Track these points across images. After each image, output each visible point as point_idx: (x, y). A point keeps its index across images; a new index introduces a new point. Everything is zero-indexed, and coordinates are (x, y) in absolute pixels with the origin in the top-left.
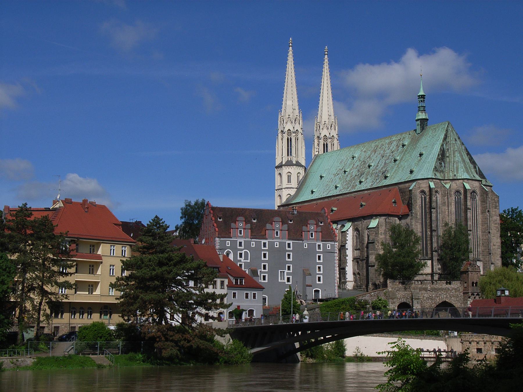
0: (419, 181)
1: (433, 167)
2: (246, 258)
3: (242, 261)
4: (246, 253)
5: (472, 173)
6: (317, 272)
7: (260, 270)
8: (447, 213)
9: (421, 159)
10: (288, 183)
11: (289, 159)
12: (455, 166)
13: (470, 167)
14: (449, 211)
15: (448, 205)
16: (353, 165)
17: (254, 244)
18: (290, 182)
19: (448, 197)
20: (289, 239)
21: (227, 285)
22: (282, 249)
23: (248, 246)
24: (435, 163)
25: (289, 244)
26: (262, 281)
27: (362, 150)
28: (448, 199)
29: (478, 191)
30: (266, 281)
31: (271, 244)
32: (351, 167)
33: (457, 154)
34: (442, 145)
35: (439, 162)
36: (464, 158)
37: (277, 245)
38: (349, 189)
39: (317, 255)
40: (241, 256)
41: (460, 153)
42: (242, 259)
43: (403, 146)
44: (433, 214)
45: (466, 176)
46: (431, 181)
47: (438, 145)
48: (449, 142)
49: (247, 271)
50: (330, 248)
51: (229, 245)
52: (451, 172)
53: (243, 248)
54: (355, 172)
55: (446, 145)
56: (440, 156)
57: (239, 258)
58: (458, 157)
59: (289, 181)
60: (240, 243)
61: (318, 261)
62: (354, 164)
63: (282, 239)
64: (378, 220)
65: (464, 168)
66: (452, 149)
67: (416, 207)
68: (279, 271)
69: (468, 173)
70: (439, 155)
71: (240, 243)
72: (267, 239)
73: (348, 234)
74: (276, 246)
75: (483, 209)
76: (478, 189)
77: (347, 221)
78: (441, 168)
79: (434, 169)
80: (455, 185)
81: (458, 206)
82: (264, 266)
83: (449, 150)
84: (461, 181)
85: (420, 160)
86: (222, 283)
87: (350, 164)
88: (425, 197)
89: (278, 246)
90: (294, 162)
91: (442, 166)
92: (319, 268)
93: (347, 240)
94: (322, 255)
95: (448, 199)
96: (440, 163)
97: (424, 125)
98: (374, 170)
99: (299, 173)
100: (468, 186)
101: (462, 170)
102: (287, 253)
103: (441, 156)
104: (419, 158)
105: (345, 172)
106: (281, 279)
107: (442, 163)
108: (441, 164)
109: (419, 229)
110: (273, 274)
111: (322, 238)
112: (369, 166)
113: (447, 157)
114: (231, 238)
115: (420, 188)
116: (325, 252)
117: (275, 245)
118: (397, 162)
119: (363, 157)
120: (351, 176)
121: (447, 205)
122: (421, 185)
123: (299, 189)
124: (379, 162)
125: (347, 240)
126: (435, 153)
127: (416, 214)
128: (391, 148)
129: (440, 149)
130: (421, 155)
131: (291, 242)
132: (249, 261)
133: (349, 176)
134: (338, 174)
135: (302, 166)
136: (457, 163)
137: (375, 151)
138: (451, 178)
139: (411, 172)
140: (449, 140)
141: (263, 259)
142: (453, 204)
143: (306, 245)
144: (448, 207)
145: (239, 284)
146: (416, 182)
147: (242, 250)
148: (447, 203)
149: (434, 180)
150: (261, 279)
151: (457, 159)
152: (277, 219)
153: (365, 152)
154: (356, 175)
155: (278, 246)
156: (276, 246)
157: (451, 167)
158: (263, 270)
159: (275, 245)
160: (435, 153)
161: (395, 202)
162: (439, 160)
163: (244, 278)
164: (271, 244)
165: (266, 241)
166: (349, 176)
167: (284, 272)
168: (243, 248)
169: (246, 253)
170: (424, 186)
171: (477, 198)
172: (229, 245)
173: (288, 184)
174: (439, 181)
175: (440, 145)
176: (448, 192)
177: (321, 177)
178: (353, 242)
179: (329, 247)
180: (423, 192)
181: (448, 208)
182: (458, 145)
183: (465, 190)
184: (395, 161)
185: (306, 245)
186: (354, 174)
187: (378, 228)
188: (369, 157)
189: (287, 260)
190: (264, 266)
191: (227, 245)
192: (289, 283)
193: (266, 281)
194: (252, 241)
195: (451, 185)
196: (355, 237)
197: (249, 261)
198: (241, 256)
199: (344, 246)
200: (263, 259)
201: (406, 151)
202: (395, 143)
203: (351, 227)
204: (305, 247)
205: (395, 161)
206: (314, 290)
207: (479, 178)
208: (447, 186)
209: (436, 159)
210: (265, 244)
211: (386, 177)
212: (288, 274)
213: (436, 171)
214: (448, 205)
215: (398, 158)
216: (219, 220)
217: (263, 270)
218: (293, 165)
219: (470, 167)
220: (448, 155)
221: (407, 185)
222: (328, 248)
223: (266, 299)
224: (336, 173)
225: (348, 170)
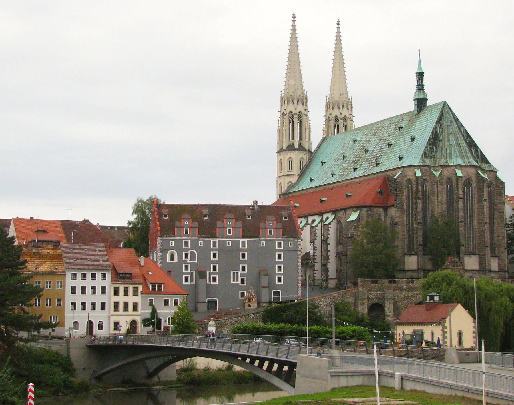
0: (406, 169)
1: (422, 153)
2: (193, 259)
4: (193, 254)
5: (468, 158)
8: (436, 203)
9: (412, 143)
10: (290, 169)
11: (291, 144)
12: (448, 151)
13: (466, 152)
14: (439, 201)
15: (438, 194)
16: (352, 150)
18: (292, 169)
19: (437, 186)
20: (244, 237)
21: (141, 292)
22: (235, 249)
23: (194, 245)
24: (424, 148)
25: (244, 243)
26: (212, 283)
27: (364, 133)
28: (437, 188)
29: (474, 178)
30: (217, 283)
31: (222, 244)
32: (350, 152)
33: (452, 138)
34: (435, 128)
35: (430, 146)
36: (460, 141)
37: (229, 243)
38: (343, 177)
39: (277, 254)
40: (187, 256)
41: (455, 136)
42: (188, 260)
43: (400, 128)
44: (418, 205)
45: (460, 162)
46: (418, 169)
47: (431, 127)
48: (444, 124)
49: (194, 273)
50: (292, 246)
52: (443, 157)
53: (189, 248)
54: (352, 158)
55: (440, 128)
56: (432, 140)
57: (184, 259)
58: (452, 141)
59: (291, 167)
60: (186, 243)
61: (277, 260)
62: (354, 149)
63: (235, 237)
64: (358, 213)
65: (458, 154)
66: (446, 132)
67: (402, 197)
69: (462, 157)
70: (430, 139)
71: (186, 243)
72: (215, 237)
73: (330, 228)
74: (227, 245)
75: (479, 198)
76: (474, 176)
77: (331, 213)
78: (432, 154)
79: (423, 155)
80: (447, 173)
81: (450, 196)
83: (443, 133)
84: (453, 168)
85: (411, 145)
86: (136, 290)
87: (351, 149)
88: (411, 186)
89: (230, 245)
90: (296, 146)
91: (434, 152)
92: (280, 268)
93: (329, 234)
94: (282, 254)
95: (437, 188)
96: (430, 148)
97: (422, 105)
98: (369, 156)
99: (302, 158)
100: (459, 173)
101: (455, 155)
102: (241, 253)
103: (433, 140)
104: (411, 142)
105: (344, 157)
106: (234, 281)
107: (433, 148)
108: (432, 149)
109: (405, 222)
110: (225, 275)
111: (283, 235)
112: (366, 151)
113: (440, 141)
115: (406, 176)
116: (287, 250)
118: (392, 146)
119: (363, 140)
120: (349, 162)
121: (436, 194)
122: (408, 173)
123: (301, 176)
124: (376, 146)
125: (329, 234)
126: (426, 137)
127: (402, 205)
128: (390, 130)
129: (432, 132)
130: (413, 139)
131: (246, 240)
133: (347, 162)
134: (338, 160)
135: (305, 150)
136: (451, 147)
137: (375, 134)
138: (442, 164)
139: (401, 158)
140: (444, 122)
141: (212, 259)
142: (444, 193)
143: (263, 244)
144: (438, 196)
145: (157, 290)
146: (402, 169)
147: (188, 250)
148: (436, 192)
149: (422, 167)
150: (210, 281)
151: (451, 143)
152: (229, 216)
153: (366, 135)
154: (353, 161)
155: (230, 245)
156: (227, 245)
157: (443, 152)
158: (212, 271)
160: (426, 137)
161: (380, 192)
162: (430, 144)
163: (163, 283)
164: (222, 244)
165: (217, 240)
166: (347, 162)
167: (237, 273)
168: (189, 248)
169: (193, 254)
170: (411, 174)
171: (473, 186)
173: (290, 170)
174: (428, 168)
175: (432, 129)
176: (437, 180)
177: (323, 163)
178: (337, 236)
179: (291, 245)
180: (409, 180)
181: (438, 198)
182: (454, 127)
183: (458, 178)
184: (390, 145)
185: (263, 244)
186: (352, 160)
187: (359, 221)
188: (369, 140)
189: (241, 259)
192: (243, 285)
193: (217, 283)
195: (441, 172)
196: (338, 231)
197: (196, 262)
198: (187, 256)
199: (326, 240)
200: (212, 259)
201: (401, 134)
202: (394, 126)
203: (334, 219)
205: (390, 145)
206: (279, 292)
207: (474, 163)
208: (437, 174)
209: (426, 143)
210: (215, 243)
211: (378, 164)
212: (242, 275)
213: (425, 157)
214: (438, 194)
215: (393, 142)
217: (212, 271)
218: (295, 150)
219: (466, 152)
220: (441, 138)
221: (395, 172)
222: (289, 246)
223: (216, 302)
224: (337, 159)
225: (347, 155)
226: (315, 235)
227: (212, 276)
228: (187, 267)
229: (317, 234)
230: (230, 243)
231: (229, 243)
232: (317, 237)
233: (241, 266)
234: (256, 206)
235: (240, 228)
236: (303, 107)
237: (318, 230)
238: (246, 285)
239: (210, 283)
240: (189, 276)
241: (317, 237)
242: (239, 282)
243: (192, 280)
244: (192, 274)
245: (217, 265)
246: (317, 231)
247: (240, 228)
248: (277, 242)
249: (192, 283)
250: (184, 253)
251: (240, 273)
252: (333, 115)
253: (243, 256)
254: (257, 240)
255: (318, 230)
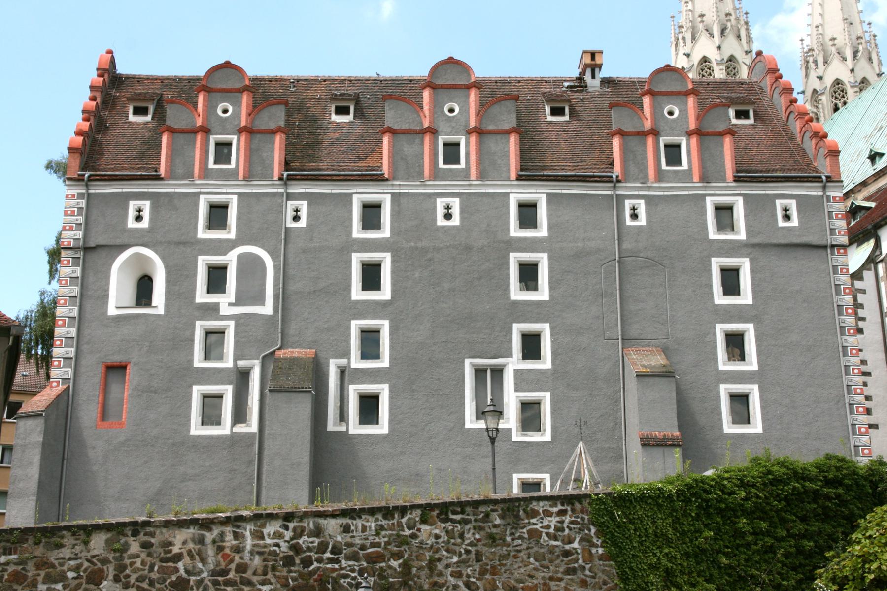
3: (225, 310)
6: (722, 367)
7: (343, 362)
17: (303, 214)
26: (355, 427)
30: (383, 427)
39: (716, 264)
51: (145, 224)
57: (202, 296)
61: (720, 299)
68: (468, 362)
74: (441, 222)
82: (370, 339)
92: (735, 342)
114: (158, 178)
117: (440, 211)
131: (538, 194)
132: (267, 309)
141: (357, 293)
150: (343, 417)
155: (456, 221)
156: (441, 222)
158: (356, 362)
159: (440, 211)
165: (382, 196)
167: (498, 372)
172: (145, 224)
189: (517, 293)
190: (370, 339)
191: (131, 224)
192: (534, 437)
193: (383, 427)
194: (290, 197)
197: (267, 309)
200: (357, 293)
204: (629, 222)
210: (371, 212)
212: (523, 380)
216: (132, 118)
217: (356, 362)
226: (856, 314)
227: (354, 391)
228: (214, 336)
229: (861, 306)
230: (456, 211)
231: (448, 208)
232: (863, 319)
233: (517, 329)
234: (593, 77)
235: (508, 132)
236: (741, 45)
237: (864, 291)
238: (547, 437)
239: (343, 429)
240: (228, 391)
241: (863, 319)
242: (511, 420)
243: (240, 415)
244: (243, 376)
245: (385, 326)
246: (861, 298)
247: (508, 132)
248: (710, 204)
249: (240, 429)
250: (203, 262)
251: (516, 372)
252: (829, 81)
253: (528, 274)
254: (602, 190)
255: (864, 291)
